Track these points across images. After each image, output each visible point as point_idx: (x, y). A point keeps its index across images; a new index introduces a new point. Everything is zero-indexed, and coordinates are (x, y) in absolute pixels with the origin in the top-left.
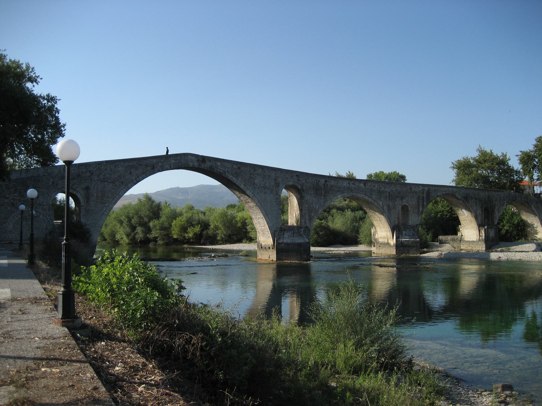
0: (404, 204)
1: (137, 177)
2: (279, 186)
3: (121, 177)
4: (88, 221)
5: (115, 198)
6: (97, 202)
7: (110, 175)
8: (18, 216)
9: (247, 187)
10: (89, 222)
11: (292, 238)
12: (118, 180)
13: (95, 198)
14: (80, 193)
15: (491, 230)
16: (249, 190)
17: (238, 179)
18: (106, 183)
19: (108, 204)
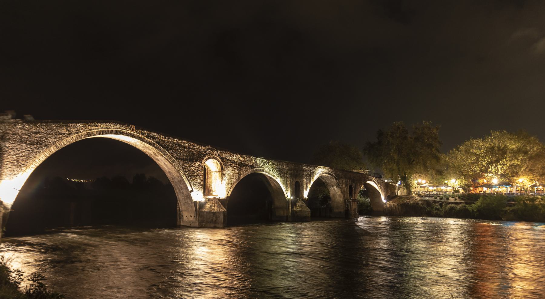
0: (297, 180)
15: (354, 203)
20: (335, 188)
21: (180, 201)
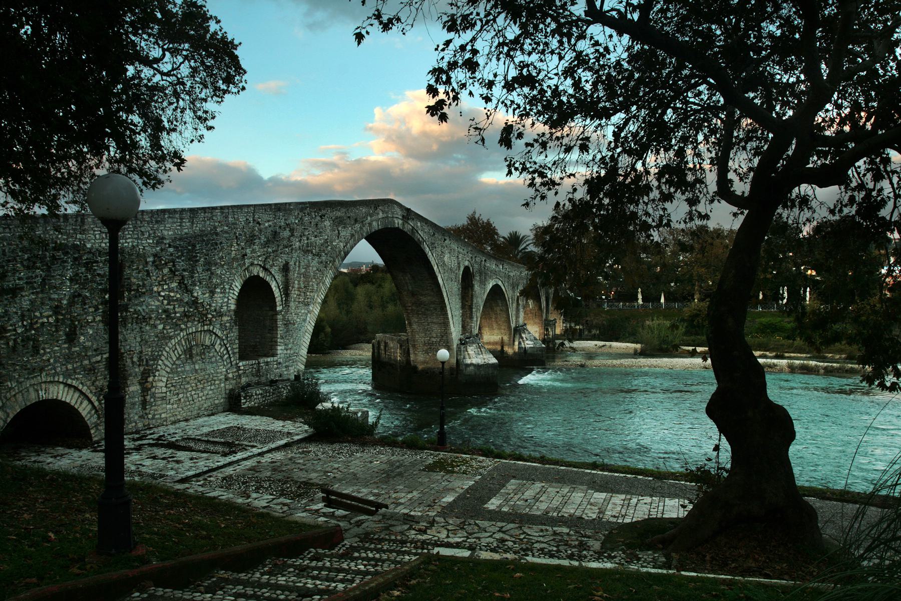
4: (287, 350)
7: (316, 237)
8: (176, 349)
10: (289, 352)
14: (275, 279)
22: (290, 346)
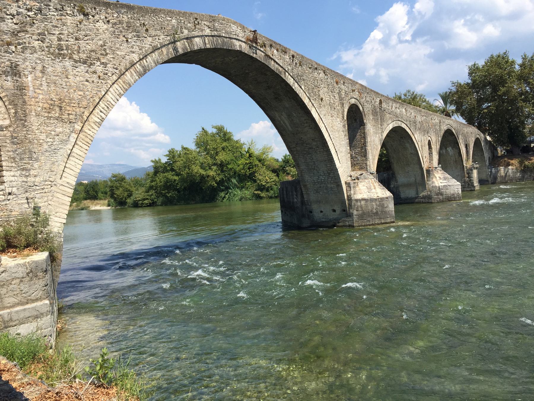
1: (143, 58)
2: (343, 104)
3: (105, 50)
5: (97, 110)
6: (49, 118)
9: (312, 103)
11: (374, 190)
12: (99, 59)
13: (41, 105)
16: (314, 109)
17: (301, 87)
18: (68, 63)
19: (79, 123)
20: (449, 151)
21: (305, 186)
22: (32, 172)
